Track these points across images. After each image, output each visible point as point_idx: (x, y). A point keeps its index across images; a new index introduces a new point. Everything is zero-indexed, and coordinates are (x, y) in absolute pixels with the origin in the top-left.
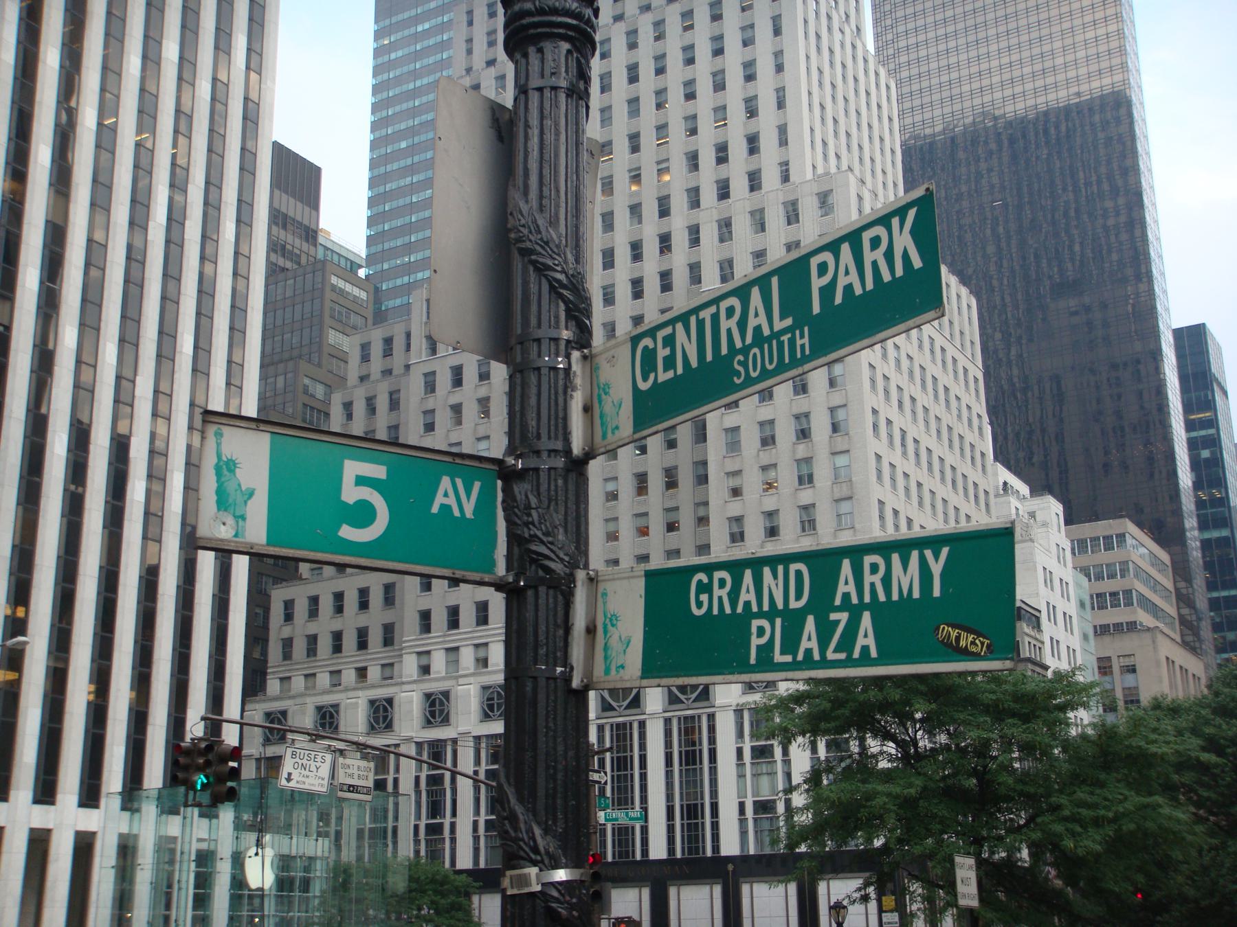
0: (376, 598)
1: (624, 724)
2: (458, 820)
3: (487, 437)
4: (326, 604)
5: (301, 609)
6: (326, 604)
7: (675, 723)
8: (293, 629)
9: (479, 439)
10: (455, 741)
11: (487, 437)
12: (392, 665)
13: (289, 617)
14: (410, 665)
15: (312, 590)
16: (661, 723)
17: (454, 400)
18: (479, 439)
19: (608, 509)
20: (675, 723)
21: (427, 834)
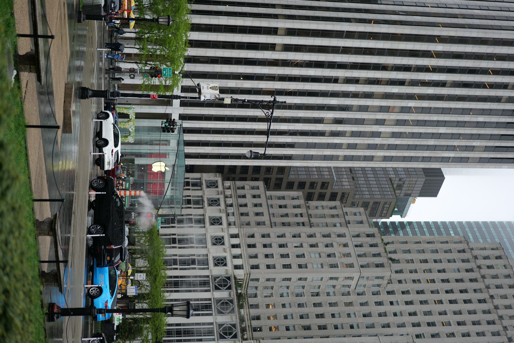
0: (259, 219)
1: (211, 308)
2: (177, 249)
3: (320, 257)
4: (257, 201)
5: (256, 192)
6: (257, 201)
7: (212, 326)
8: (247, 190)
9: (319, 254)
10: (206, 247)
11: (320, 257)
12: (235, 225)
13: (253, 188)
14: (234, 230)
15: (263, 196)
16: (211, 321)
17: (335, 244)
18: (319, 254)
19: (294, 304)
20: (212, 326)
21: (172, 238)
